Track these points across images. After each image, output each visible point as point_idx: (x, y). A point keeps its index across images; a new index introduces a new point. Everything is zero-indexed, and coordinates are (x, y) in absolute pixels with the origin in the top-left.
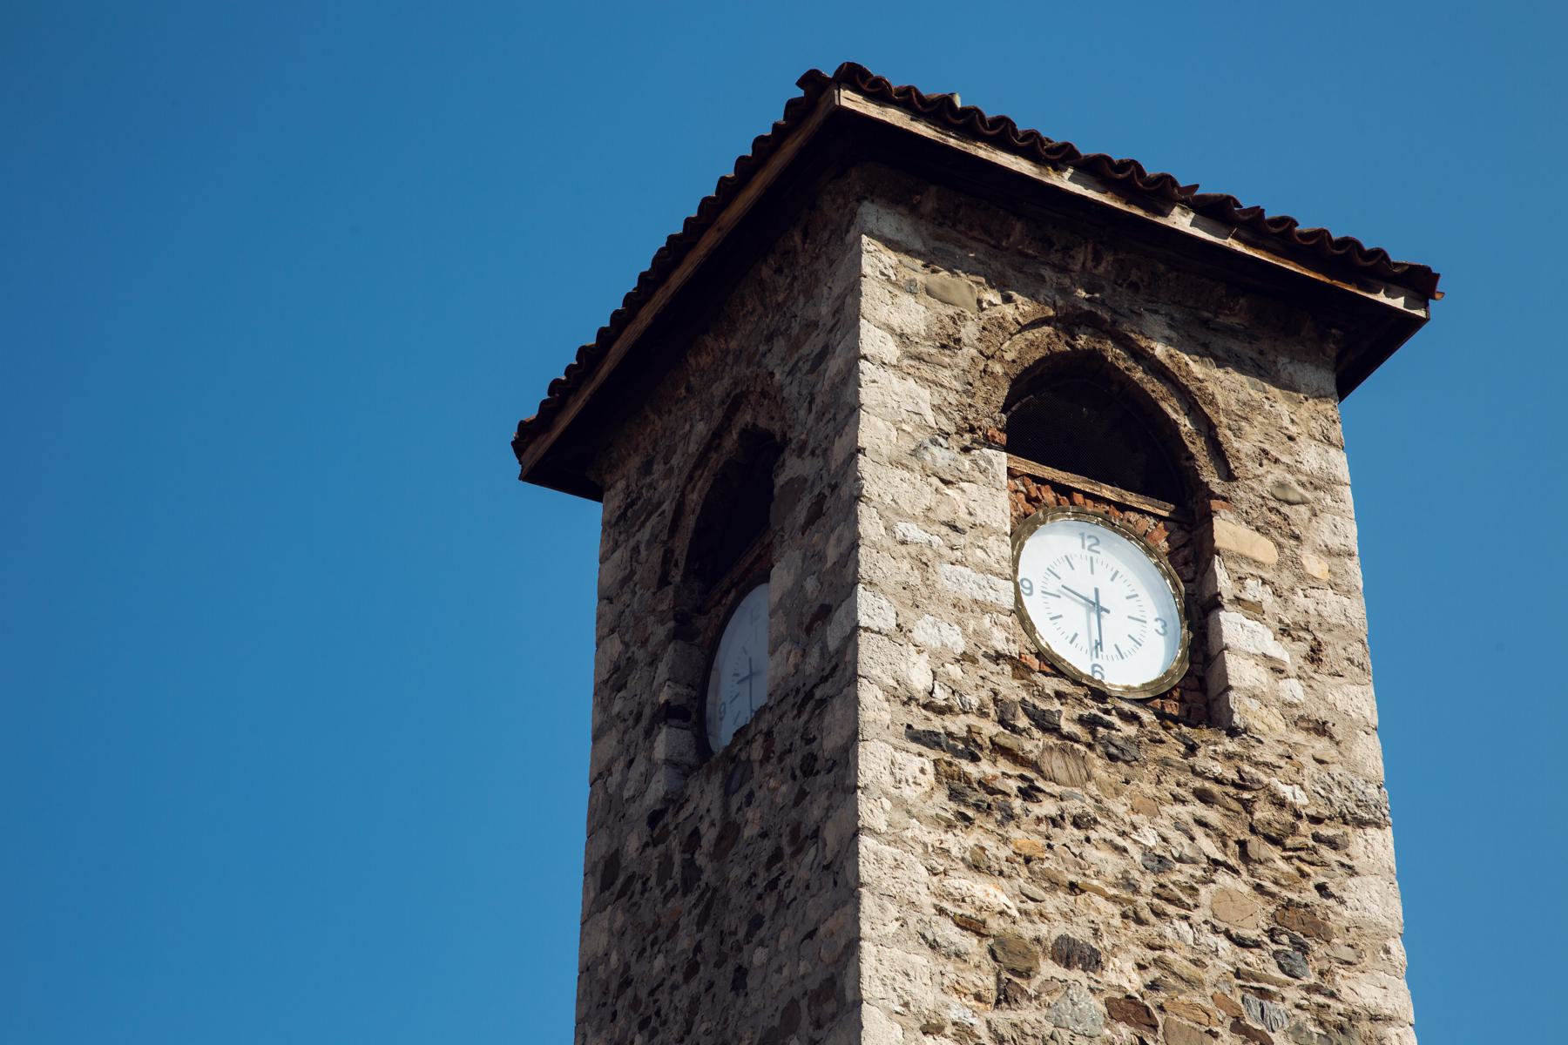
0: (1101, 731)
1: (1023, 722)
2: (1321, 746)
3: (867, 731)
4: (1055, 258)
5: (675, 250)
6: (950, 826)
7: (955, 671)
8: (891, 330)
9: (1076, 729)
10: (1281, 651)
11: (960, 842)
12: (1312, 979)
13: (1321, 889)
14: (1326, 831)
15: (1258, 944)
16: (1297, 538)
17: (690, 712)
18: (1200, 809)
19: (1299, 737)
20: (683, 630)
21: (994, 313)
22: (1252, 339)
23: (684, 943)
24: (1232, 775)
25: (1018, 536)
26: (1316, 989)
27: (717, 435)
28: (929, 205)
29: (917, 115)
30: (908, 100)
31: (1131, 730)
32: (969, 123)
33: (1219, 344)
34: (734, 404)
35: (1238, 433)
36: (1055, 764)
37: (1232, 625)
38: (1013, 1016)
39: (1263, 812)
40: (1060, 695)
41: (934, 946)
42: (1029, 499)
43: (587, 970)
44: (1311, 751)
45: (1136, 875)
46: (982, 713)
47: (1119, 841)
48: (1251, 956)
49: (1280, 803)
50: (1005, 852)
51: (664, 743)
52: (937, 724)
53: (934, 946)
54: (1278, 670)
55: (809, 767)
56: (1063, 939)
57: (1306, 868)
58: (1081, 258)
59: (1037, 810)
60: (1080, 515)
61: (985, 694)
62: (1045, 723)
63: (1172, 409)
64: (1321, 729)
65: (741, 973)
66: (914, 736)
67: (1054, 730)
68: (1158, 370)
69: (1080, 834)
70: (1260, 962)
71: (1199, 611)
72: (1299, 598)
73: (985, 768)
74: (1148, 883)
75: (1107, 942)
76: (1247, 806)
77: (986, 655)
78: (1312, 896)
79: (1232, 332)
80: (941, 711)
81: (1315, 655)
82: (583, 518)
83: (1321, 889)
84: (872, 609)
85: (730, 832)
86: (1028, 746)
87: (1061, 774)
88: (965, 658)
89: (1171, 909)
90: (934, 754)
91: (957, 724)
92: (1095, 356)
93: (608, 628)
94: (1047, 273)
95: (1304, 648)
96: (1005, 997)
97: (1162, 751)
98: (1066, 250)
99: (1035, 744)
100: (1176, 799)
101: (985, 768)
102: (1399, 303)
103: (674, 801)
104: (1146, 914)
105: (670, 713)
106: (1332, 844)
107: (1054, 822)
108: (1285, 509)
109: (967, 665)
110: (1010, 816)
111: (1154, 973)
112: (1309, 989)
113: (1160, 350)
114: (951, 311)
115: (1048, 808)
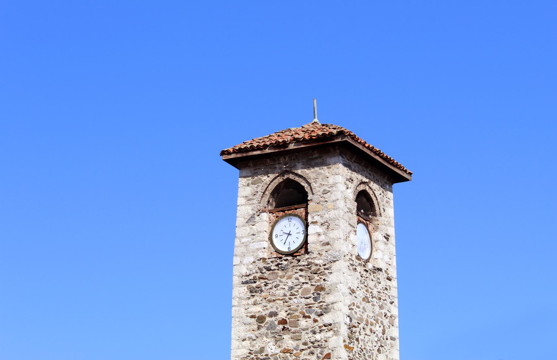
0: (280, 266)
1: (264, 270)
2: (328, 247)
3: (234, 286)
4: (277, 162)
6: (249, 298)
7: (251, 266)
8: (244, 197)
9: (276, 268)
12: (321, 299)
13: (324, 280)
14: (326, 267)
15: (310, 297)
16: (326, 201)
18: (301, 273)
21: (265, 182)
22: (320, 157)
24: (306, 263)
26: (321, 302)
28: (251, 164)
29: (237, 153)
30: (234, 152)
31: (285, 263)
32: (246, 150)
33: (313, 163)
35: (315, 182)
36: (271, 277)
37: (311, 229)
38: (259, 332)
39: (314, 268)
40: (272, 262)
42: (277, 217)
44: (325, 250)
45: (286, 293)
46: (257, 273)
47: (284, 287)
48: (308, 300)
49: (317, 265)
50: (261, 299)
52: (248, 279)
56: (271, 312)
57: (321, 277)
58: (282, 160)
59: (267, 287)
60: (286, 216)
61: (257, 269)
62: (269, 269)
63: (303, 184)
64: (328, 244)
66: (243, 283)
67: (270, 270)
68: (300, 176)
69: (276, 289)
70: (311, 301)
72: (327, 216)
74: (288, 294)
75: (279, 310)
76: (310, 268)
77: (258, 260)
78: (322, 282)
79: (316, 158)
80: (248, 276)
83: (324, 280)
84: (236, 260)
86: (265, 275)
87: (272, 278)
88: (254, 262)
89: (293, 297)
90: (247, 285)
92: (288, 179)
94: (277, 166)
95: (326, 226)
96: (259, 328)
97: (293, 264)
98: (279, 160)
99: (267, 274)
100: (296, 273)
101: (258, 283)
102: (340, 140)
104: (288, 300)
106: (327, 269)
108: (325, 195)
109: (254, 264)
110: (262, 291)
111: (289, 312)
112: (319, 303)
113: (299, 172)
114: (256, 186)
115: (270, 286)
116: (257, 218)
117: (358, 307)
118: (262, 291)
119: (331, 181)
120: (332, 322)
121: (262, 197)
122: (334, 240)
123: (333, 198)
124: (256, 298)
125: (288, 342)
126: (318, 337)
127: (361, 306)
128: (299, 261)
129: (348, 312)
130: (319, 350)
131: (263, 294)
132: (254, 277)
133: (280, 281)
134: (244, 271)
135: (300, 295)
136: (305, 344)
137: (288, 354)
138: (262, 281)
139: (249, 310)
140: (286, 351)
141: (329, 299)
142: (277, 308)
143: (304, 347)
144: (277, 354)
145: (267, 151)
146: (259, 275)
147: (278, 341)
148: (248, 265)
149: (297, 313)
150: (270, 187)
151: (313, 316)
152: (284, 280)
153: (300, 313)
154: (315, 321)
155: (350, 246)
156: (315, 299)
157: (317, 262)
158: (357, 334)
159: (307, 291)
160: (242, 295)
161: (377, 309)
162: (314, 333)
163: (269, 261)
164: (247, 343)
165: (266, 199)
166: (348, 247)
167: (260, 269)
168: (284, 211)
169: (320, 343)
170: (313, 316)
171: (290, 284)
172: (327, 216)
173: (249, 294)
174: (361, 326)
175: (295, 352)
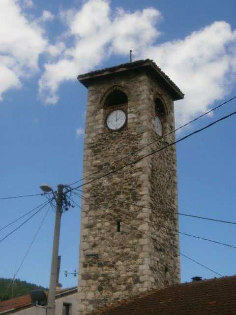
2: (139, 125)
6: (93, 156)
7: (94, 138)
10: (134, 116)
11: (94, 158)
12: (135, 154)
13: (137, 143)
19: (136, 126)
31: (115, 135)
37: (130, 116)
39: (131, 137)
41: (91, 170)
49: (133, 135)
52: (92, 145)
53: (91, 170)
54: (134, 118)
62: (105, 139)
64: (139, 123)
66: (90, 148)
74: (116, 152)
76: (129, 137)
78: (136, 144)
81: (139, 115)
83: (137, 143)
88: (96, 136)
91: (95, 144)
106: (139, 137)
107: (106, 150)
115: (105, 148)
116: (98, 112)
117: (156, 160)
118: (100, 152)
119: (141, 89)
120: (142, 166)
121: (101, 101)
122: (143, 121)
123: (142, 98)
124: (97, 156)
125: (116, 179)
126: (133, 175)
127: (158, 160)
128: (122, 134)
129: (151, 162)
130: (134, 182)
131: (101, 153)
132: (96, 144)
133: (112, 146)
135: (123, 152)
136: (126, 179)
137: (116, 186)
138: (101, 146)
139: (93, 162)
141: (140, 154)
142: (109, 161)
143: (125, 181)
144: (109, 186)
145: (105, 74)
146: (98, 143)
147: (109, 179)
148: (92, 138)
149: (121, 163)
150: (105, 96)
152: (113, 145)
153: (123, 162)
155: (152, 126)
157: (132, 133)
158: (156, 175)
159: (127, 150)
160: (89, 154)
161: (166, 165)
162: (131, 173)
163: (104, 135)
165: (103, 102)
166: (151, 126)
168: (113, 108)
169: (134, 179)
171: (117, 147)
172: (139, 108)
173: (93, 154)
174: (158, 171)
175: (120, 184)
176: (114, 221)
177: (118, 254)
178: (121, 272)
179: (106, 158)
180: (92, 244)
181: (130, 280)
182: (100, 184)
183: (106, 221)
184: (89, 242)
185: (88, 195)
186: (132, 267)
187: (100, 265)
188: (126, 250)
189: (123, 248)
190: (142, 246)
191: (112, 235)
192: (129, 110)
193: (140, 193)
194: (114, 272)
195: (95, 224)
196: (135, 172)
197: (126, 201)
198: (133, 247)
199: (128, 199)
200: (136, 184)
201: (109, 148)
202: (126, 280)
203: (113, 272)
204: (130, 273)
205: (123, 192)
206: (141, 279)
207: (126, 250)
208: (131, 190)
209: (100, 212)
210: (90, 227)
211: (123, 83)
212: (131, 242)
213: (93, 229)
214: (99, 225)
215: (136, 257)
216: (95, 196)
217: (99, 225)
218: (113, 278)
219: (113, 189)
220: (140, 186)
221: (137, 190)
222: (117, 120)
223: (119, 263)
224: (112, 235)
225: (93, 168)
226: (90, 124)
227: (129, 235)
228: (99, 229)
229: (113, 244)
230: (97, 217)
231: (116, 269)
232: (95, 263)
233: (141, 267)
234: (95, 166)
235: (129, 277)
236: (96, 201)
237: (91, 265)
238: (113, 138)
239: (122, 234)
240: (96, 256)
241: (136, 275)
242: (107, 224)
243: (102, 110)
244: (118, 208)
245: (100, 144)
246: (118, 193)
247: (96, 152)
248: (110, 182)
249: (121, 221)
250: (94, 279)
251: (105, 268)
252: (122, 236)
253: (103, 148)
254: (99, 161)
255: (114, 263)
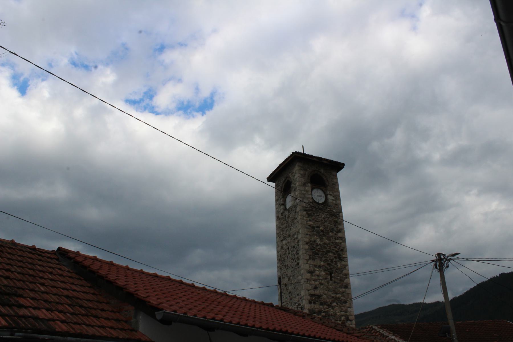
5: (281, 165)
11: (308, 219)
17: (284, 204)
20: (283, 197)
23: (285, 225)
25: (312, 191)
27: (285, 180)
34: (287, 177)
37: (329, 197)
43: (277, 225)
51: (282, 207)
54: (333, 200)
55: (296, 212)
62: (315, 208)
63: (324, 177)
65: (291, 229)
70: (333, 225)
71: (326, 196)
73: (310, 212)
81: (336, 198)
82: (273, 184)
85: (289, 217)
93: (276, 195)
99: (314, 210)
101: (310, 212)
103: (283, 212)
105: (282, 204)
126: (337, 241)
134: (304, 205)
136: (333, 243)
140: (325, 244)
141: (340, 227)
145: (315, 159)
147: (321, 239)
149: (328, 229)
151: (335, 232)
154: (335, 234)
156: (335, 226)
162: (336, 239)
164: (308, 236)
167: (311, 207)
170: (335, 232)
171: (323, 216)
173: (307, 216)
176: (327, 272)
177: (333, 297)
178: (337, 311)
179: (316, 223)
180: (314, 286)
181: (343, 318)
182: (315, 241)
183: (321, 271)
184: (311, 285)
185: (307, 247)
186: (344, 308)
187: (321, 304)
188: (338, 295)
189: (336, 294)
190: (348, 294)
191: (328, 282)
192: (328, 192)
193: (343, 256)
194: (332, 310)
195: (315, 271)
196: (338, 239)
197: (335, 259)
198: (342, 293)
199: (335, 257)
200: (339, 248)
201: (318, 216)
202: (341, 318)
203: (331, 311)
204: (343, 313)
205: (332, 252)
206: (350, 318)
207: (338, 295)
208: (337, 251)
209: (318, 262)
210: (311, 272)
211: (322, 171)
212: (341, 290)
213: (313, 274)
214: (317, 273)
215: (345, 302)
216: (312, 249)
217: (317, 273)
218: (332, 315)
219: (325, 248)
220: (342, 250)
221: (341, 253)
222: (318, 196)
223: (334, 304)
224: (328, 282)
225: (309, 227)
226: (303, 192)
227: (339, 285)
228: (318, 276)
229: (329, 290)
230: (315, 266)
231: (333, 309)
232: (317, 301)
233: (349, 309)
234: (310, 226)
235: (343, 316)
236: (313, 252)
237: (314, 303)
238: (321, 209)
239: (335, 282)
240: (319, 296)
241: (346, 315)
242: (323, 273)
243: (309, 184)
244: (329, 262)
245: (311, 210)
246: (329, 252)
247: (309, 215)
248: (322, 241)
249: (332, 273)
250: (318, 314)
251: (325, 306)
252: (334, 285)
253: (314, 214)
254: (311, 223)
255: (331, 303)
